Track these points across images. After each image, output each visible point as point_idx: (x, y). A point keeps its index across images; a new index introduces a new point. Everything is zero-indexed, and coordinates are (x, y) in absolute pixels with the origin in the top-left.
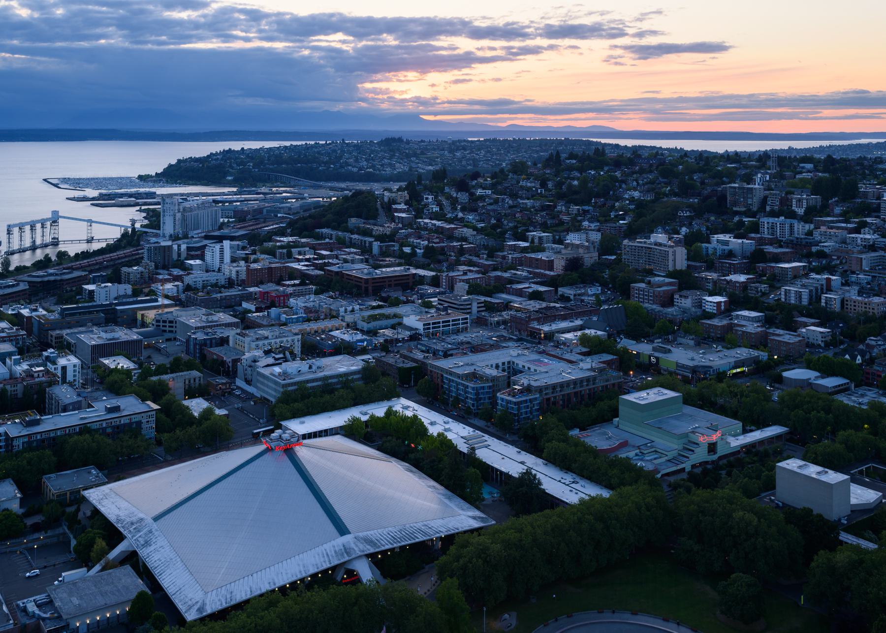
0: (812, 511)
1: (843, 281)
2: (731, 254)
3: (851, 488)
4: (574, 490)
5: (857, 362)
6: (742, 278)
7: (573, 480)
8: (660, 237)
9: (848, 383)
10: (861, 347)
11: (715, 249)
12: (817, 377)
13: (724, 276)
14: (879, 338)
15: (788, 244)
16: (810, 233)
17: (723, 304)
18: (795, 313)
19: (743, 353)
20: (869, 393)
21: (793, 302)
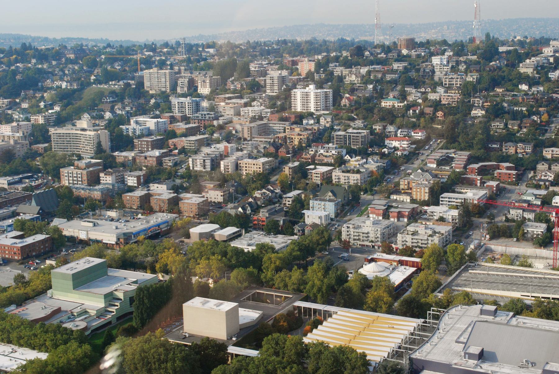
2: (150, 133)
3: (240, 312)
4: (12, 359)
7: (11, 350)
8: (84, 122)
9: (238, 231)
10: (250, 200)
11: (134, 129)
17: (142, 177)
20: (256, 236)
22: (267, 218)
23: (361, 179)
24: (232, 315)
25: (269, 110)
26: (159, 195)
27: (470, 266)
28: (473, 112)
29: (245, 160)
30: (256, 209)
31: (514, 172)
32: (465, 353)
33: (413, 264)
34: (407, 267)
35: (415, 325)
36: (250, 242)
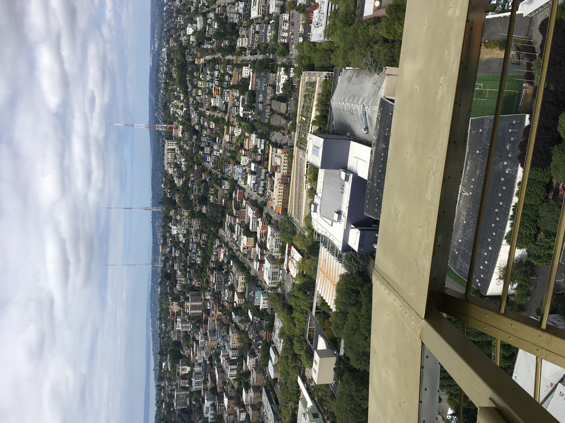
0: (334, 368)
1: (223, 348)
2: (213, 405)
5: (261, 342)
6: (226, 400)
10: (254, 341)
11: (211, 415)
12: (272, 361)
13: (226, 409)
14: (249, 333)
15: (206, 375)
16: (200, 364)
17: (241, 409)
18: (241, 372)
19: (265, 399)
20: (275, 338)
21: (236, 373)
22: (264, 331)
23: (242, 275)
24: (322, 354)
25: (201, 329)
26: (251, 398)
27: (290, 216)
28: (204, 212)
29: (231, 344)
30: (260, 338)
31: (238, 191)
32: (338, 221)
33: (290, 247)
34: (292, 250)
35: (323, 248)
36: (279, 341)
